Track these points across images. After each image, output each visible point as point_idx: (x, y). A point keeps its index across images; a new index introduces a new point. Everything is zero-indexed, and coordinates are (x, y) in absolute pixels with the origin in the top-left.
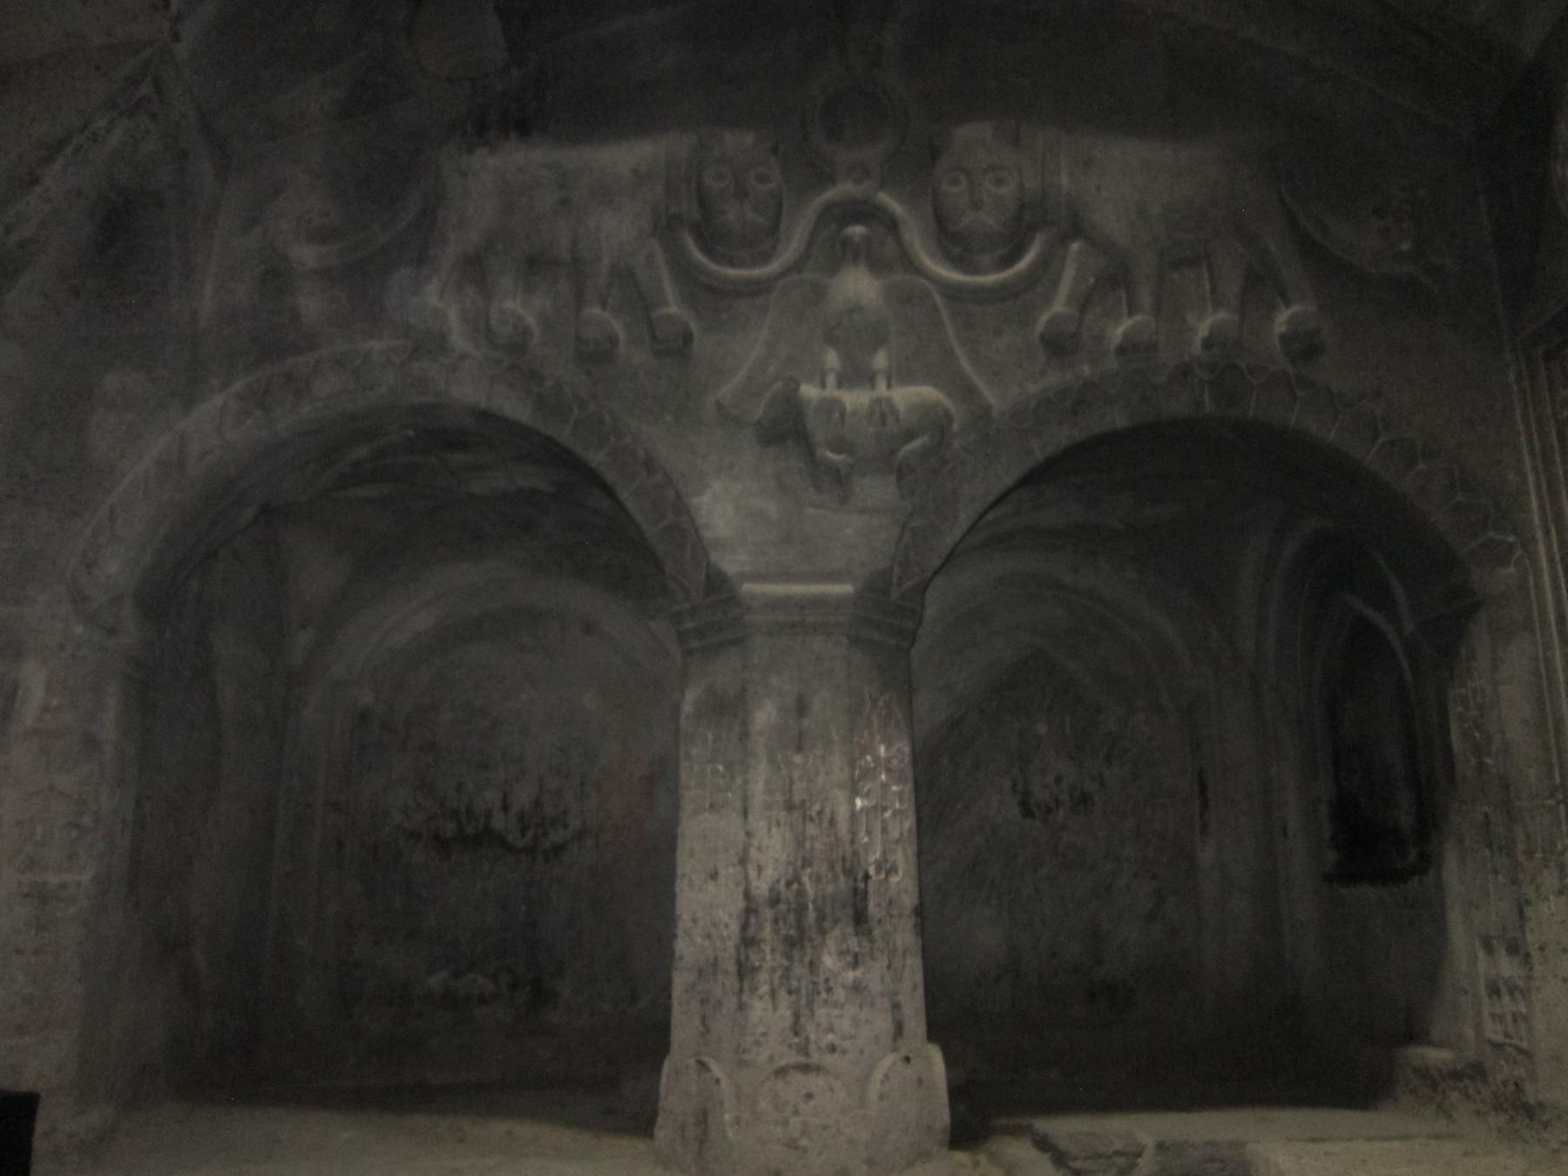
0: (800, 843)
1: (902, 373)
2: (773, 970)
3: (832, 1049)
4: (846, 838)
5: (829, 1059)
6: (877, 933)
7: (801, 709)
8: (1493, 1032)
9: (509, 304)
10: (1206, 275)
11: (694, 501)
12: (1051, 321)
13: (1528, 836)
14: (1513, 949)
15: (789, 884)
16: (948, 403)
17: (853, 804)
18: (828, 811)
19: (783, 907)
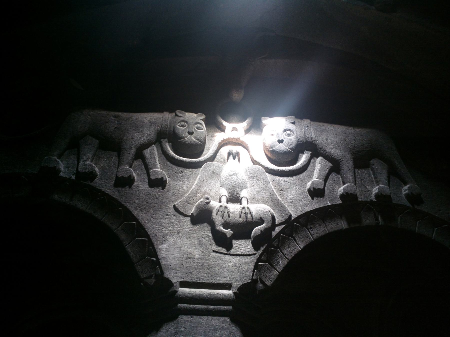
9: (89, 162)
10: (371, 172)
11: (160, 247)
12: (313, 183)
16: (272, 211)
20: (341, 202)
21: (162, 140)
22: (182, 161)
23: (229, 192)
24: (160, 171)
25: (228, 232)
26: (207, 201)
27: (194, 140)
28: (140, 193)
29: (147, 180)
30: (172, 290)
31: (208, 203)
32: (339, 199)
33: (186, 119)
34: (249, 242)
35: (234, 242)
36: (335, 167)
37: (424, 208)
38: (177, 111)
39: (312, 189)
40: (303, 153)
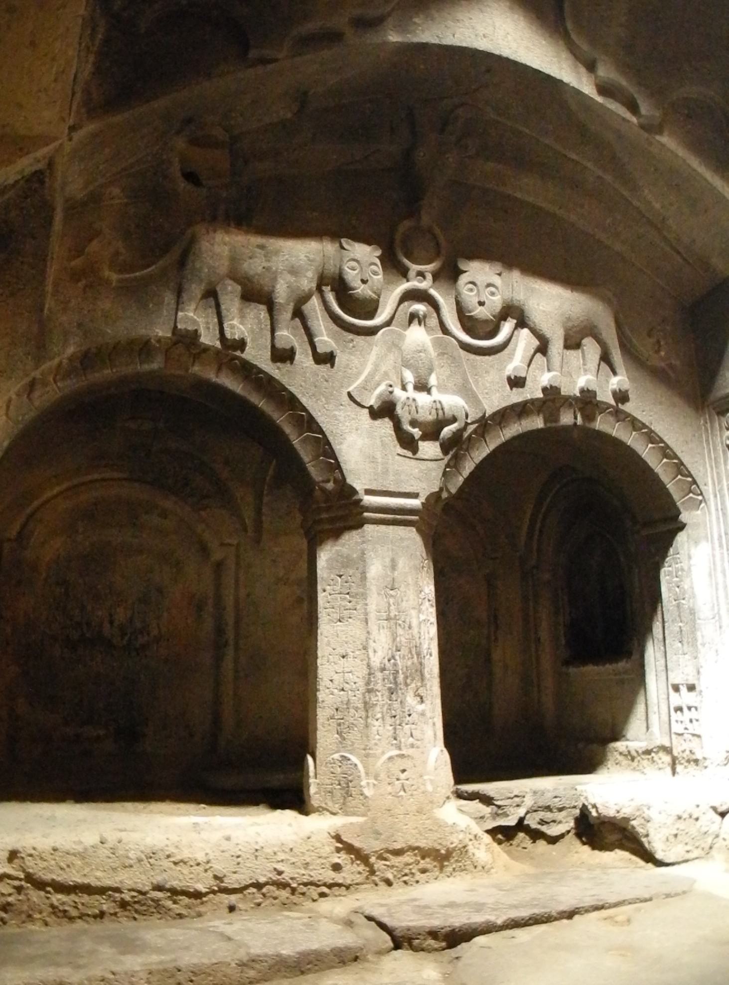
0: (394, 640)
1: (442, 388)
2: (383, 705)
3: (412, 746)
4: (417, 636)
5: (410, 752)
6: (428, 686)
7: (394, 567)
8: (677, 728)
9: (235, 322)
12: (515, 369)
13: (703, 636)
14: (691, 688)
15: (389, 660)
16: (466, 407)
17: (419, 618)
18: (407, 620)
19: (387, 672)
20: (541, 395)
21: (324, 288)
22: (353, 325)
23: (415, 377)
24: (326, 342)
25: (416, 432)
26: (390, 389)
27: (370, 293)
28: (305, 372)
29: (310, 352)
30: (355, 497)
31: (391, 393)
32: (540, 391)
33: (358, 256)
34: (437, 444)
35: (420, 443)
36: (543, 348)
37: (628, 407)
38: (343, 241)
39: (513, 377)
40: (505, 320)
